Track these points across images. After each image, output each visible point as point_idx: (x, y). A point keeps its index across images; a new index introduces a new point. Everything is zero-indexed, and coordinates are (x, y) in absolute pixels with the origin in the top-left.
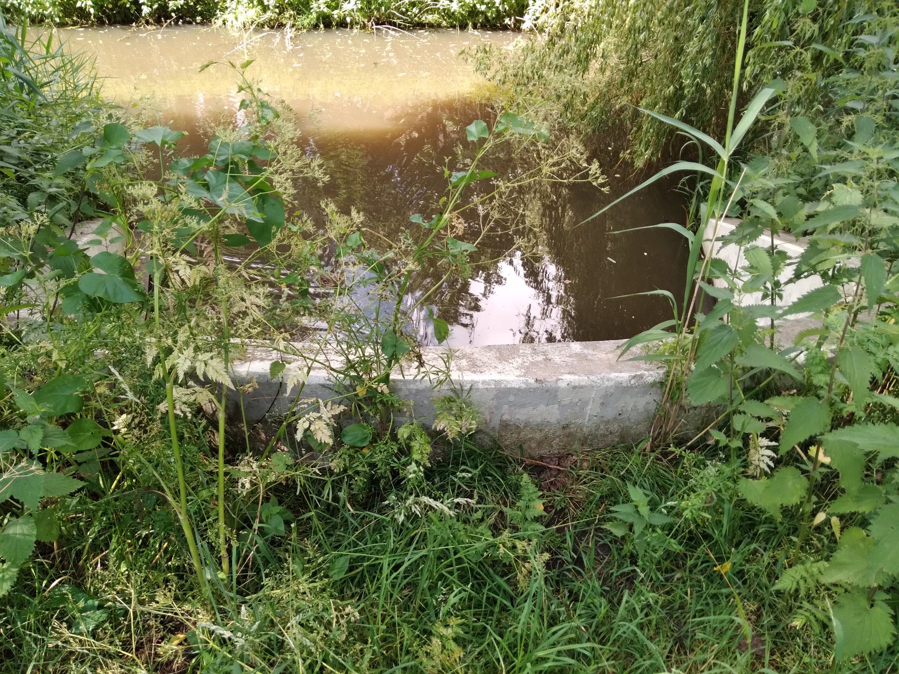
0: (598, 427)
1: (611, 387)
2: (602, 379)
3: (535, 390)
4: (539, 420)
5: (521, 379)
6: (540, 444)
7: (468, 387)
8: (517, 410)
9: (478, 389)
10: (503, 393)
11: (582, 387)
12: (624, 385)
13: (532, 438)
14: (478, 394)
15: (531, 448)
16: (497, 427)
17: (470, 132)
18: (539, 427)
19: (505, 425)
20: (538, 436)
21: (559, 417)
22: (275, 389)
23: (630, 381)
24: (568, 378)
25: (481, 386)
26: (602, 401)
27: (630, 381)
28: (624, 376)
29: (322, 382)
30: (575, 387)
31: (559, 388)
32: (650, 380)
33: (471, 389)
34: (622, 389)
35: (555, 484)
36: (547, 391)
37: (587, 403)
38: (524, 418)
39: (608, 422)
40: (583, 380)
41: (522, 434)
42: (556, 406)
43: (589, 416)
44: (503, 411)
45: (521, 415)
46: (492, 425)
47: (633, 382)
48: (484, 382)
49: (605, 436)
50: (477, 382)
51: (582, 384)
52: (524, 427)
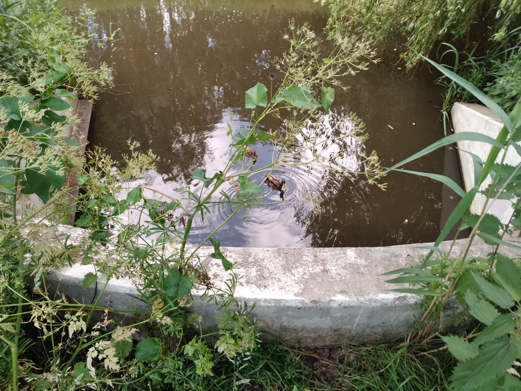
0: (364, 331)
1: (377, 307)
2: (370, 301)
3: (310, 308)
4: (314, 326)
5: (299, 298)
6: (314, 340)
7: (251, 304)
8: (295, 320)
9: (260, 306)
10: (281, 309)
11: (352, 307)
12: (389, 305)
13: (308, 337)
14: (260, 309)
15: (307, 342)
16: (278, 329)
17: (250, 98)
18: (315, 330)
19: (285, 329)
20: (313, 335)
21: (331, 324)
22: (94, 291)
23: (394, 302)
24: (340, 298)
25: (262, 304)
26: (368, 315)
27: (394, 302)
28: (390, 297)
29: (128, 292)
30: (345, 307)
31: (331, 307)
32: (412, 301)
33: (254, 306)
34: (386, 308)
35: (325, 375)
36: (321, 309)
37: (356, 317)
38: (301, 325)
39: (373, 327)
40: (353, 301)
41: (299, 334)
42: (329, 318)
43: (356, 325)
44: (282, 321)
45: (298, 323)
46: (274, 328)
47: (397, 303)
48: (265, 300)
49: (369, 335)
50: (259, 300)
51: (351, 305)
52: (301, 330)
